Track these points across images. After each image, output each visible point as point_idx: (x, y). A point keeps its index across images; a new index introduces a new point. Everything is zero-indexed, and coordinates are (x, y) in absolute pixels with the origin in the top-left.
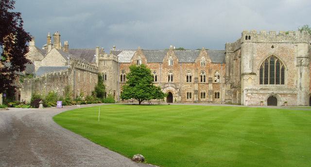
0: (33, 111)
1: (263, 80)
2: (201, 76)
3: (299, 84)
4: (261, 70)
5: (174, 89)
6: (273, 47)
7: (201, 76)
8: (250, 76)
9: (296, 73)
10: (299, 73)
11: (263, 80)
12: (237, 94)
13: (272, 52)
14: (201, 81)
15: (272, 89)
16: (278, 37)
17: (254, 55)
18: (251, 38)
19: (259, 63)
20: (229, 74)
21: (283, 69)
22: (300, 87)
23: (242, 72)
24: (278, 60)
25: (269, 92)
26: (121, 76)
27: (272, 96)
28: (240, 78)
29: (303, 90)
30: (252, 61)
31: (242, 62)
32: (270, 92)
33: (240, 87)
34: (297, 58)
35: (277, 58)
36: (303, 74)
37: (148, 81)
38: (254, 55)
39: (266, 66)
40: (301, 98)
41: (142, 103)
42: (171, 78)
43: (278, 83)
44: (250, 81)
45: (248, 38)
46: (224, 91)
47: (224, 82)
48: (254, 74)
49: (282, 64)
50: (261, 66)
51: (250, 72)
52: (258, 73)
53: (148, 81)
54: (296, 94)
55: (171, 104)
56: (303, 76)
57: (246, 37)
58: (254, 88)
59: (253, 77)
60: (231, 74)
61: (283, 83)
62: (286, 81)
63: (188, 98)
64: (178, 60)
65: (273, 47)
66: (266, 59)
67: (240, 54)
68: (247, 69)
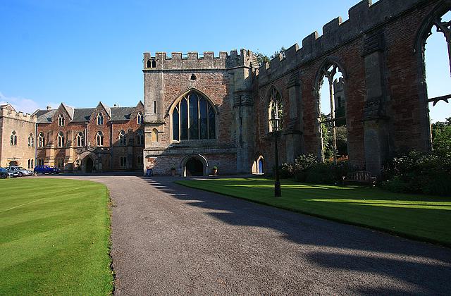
2: (139, 137)
3: (238, 136)
6: (193, 78)
7: (139, 137)
9: (234, 119)
10: (237, 118)
13: (193, 85)
14: (139, 143)
16: (202, 62)
22: (241, 140)
25: (187, 152)
27: (194, 159)
29: (245, 145)
34: (234, 93)
36: (244, 119)
40: (242, 160)
54: (234, 154)
56: (245, 125)
62: (217, 136)
63: (122, 165)
65: (193, 78)
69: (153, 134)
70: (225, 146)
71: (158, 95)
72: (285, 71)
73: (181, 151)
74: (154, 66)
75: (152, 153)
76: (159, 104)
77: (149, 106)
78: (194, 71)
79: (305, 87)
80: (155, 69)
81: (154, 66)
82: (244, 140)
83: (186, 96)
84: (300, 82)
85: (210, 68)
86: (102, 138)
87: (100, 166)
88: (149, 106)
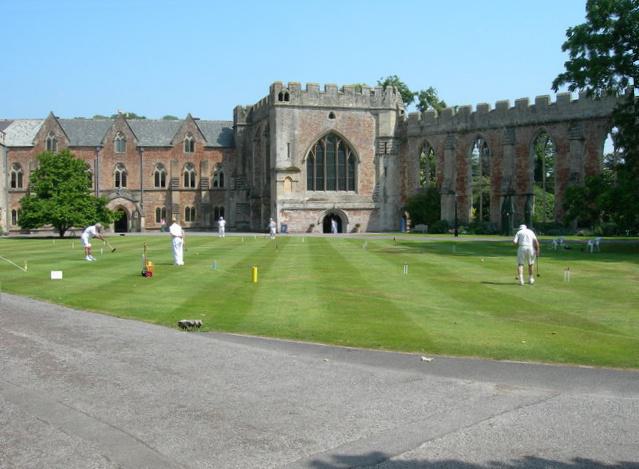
0: (192, 237)
1: (316, 182)
3: (381, 188)
4: (310, 159)
6: (332, 116)
11: (316, 182)
12: (262, 212)
13: (331, 125)
15: (333, 199)
16: (342, 98)
17: (296, 132)
18: (291, 97)
19: (304, 149)
20: (244, 170)
23: (272, 167)
24: (341, 142)
26: (157, 175)
28: (269, 179)
29: (390, 200)
30: (289, 145)
31: (271, 147)
32: (329, 206)
33: (269, 197)
35: (339, 138)
37: (78, 187)
38: (296, 132)
39: (321, 160)
40: (386, 216)
41: (67, 234)
42: (121, 180)
45: (284, 97)
46: (233, 205)
47: (232, 186)
49: (349, 150)
50: (310, 154)
52: (304, 168)
53: (78, 187)
55: (126, 234)
57: (280, 95)
58: (296, 198)
60: (247, 170)
61: (353, 187)
62: (359, 186)
65: (332, 116)
66: (320, 141)
67: (268, 129)
68: (282, 160)
69: (287, 182)
71: (292, 135)
72: (440, 129)
74: (287, 99)
75: (287, 206)
76: (294, 146)
78: (333, 108)
79: (460, 152)
80: (287, 103)
81: (287, 99)
82: (389, 193)
83: (324, 138)
84: (455, 146)
85: (351, 105)
86: (124, 175)
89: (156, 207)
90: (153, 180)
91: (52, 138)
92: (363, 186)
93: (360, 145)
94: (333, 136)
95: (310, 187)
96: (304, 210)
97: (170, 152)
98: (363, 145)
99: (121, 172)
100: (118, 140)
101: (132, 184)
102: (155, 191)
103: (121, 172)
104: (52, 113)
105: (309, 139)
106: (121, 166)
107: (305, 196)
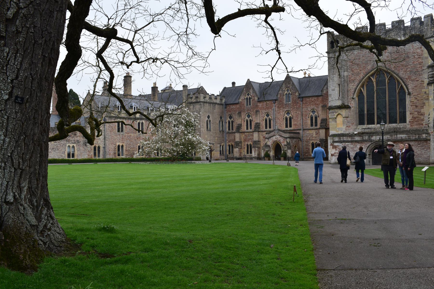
5: (282, 140)
8: (339, 111)
9: (428, 99)
21: (403, 93)
25: (374, 138)
42: (289, 122)
43: (393, 120)
44: (340, 119)
48: (347, 107)
50: (361, 92)
51: (339, 103)
52: (354, 104)
59: (344, 112)
61: (403, 120)
64: (297, 94)
66: (369, 78)
70: (415, 132)
73: (366, 138)
77: (333, 90)
83: (372, 75)
87: (289, 153)
88: (333, 90)
89: (311, 142)
90: (309, 122)
91: (248, 97)
92: (414, 118)
93: (409, 77)
94: (379, 72)
95: (361, 122)
96: (351, 142)
97: (320, 99)
98: (413, 78)
99: (288, 117)
100: (286, 94)
101: (295, 125)
102: (310, 129)
103: (288, 117)
104: (248, 80)
105: (358, 78)
106: (288, 113)
107: (355, 130)
